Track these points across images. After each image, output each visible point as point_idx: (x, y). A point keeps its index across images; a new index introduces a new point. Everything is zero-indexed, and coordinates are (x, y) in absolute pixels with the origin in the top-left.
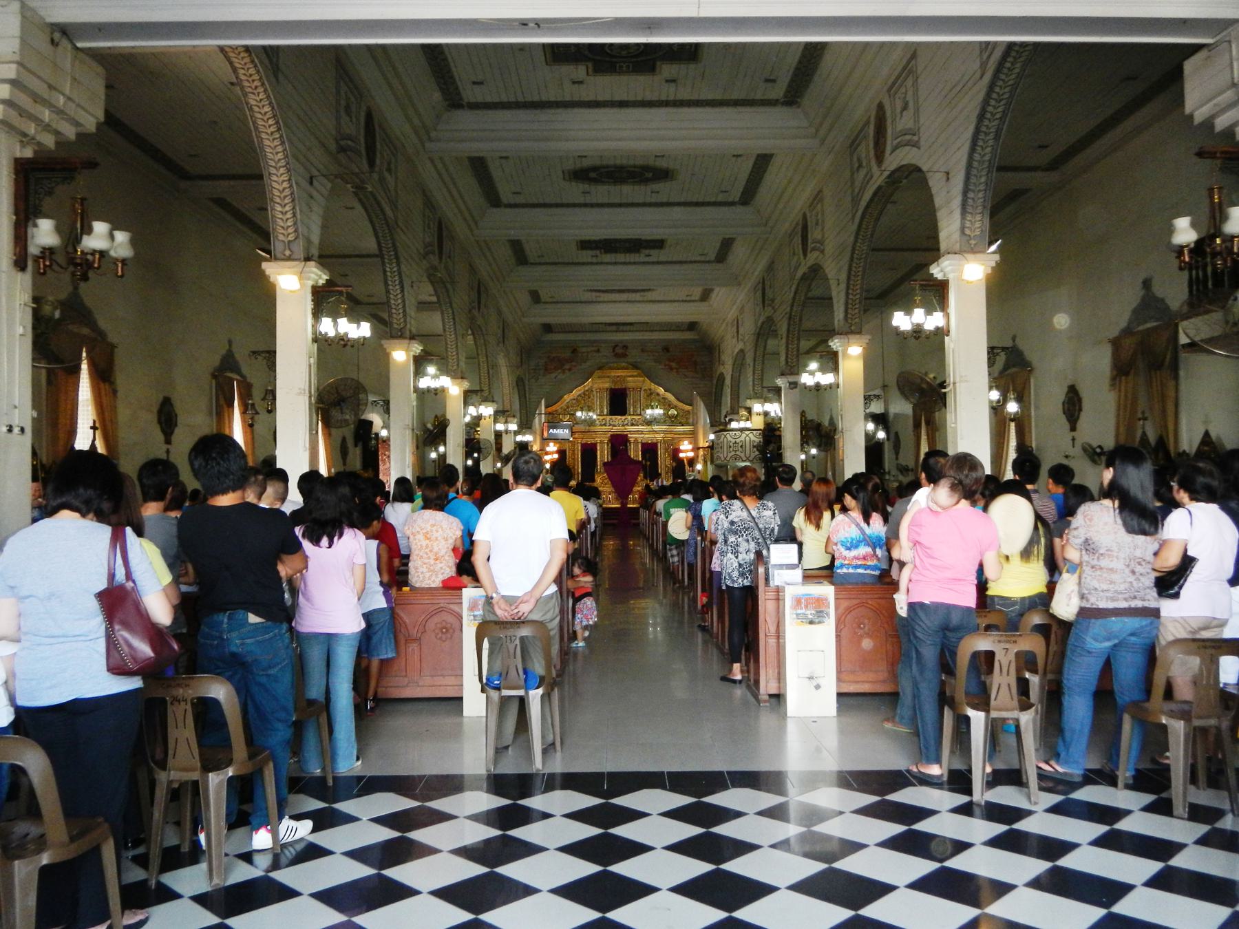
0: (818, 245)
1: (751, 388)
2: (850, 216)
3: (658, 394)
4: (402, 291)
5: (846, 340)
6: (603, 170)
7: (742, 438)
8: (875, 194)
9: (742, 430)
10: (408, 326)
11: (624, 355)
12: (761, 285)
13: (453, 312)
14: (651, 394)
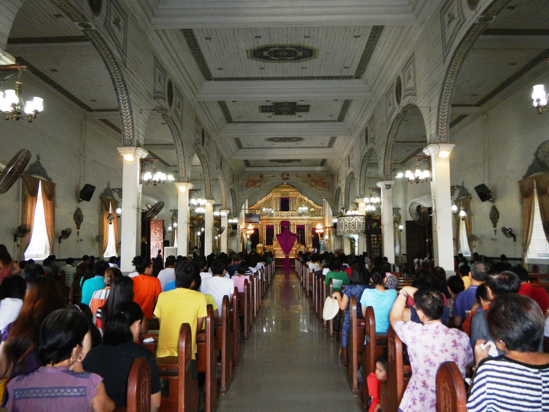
0: (411, 91)
1: (358, 192)
2: (442, 59)
3: (305, 201)
4: (131, 114)
5: (438, 148)
6: (272, 49)
7: (353, 221)
8: (468, 32)
9: (353, 216)
10: (136, 138)
11: (287, 179)
12: (365, 132)
13: (182, 142)
14: (301, 200)
